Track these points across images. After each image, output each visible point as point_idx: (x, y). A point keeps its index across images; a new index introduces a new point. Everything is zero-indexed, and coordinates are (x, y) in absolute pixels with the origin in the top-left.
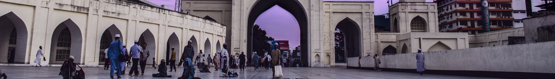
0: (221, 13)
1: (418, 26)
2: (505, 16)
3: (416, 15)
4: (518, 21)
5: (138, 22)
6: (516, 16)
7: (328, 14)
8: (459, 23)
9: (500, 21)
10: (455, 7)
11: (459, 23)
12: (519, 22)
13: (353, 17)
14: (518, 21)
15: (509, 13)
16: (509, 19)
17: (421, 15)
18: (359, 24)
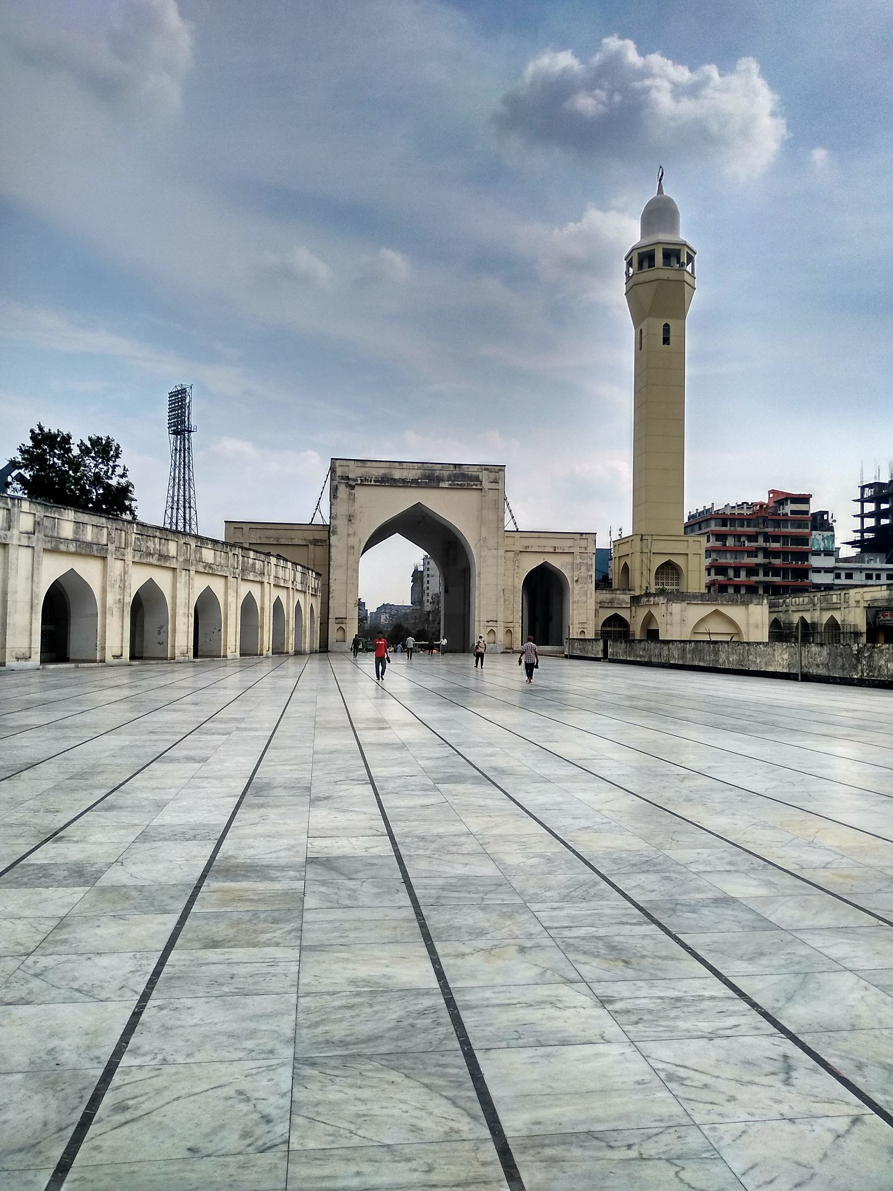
0: (306, 548)
1: (667, 579)
2: (797, 560)
3: (664, 559)
4: (818, 570)
5: (192, 573)
6: (816, 562)
7: (511, 554)
8: (713, 572)
9: (786, 570)
10: (708, 541)
11: (713, 572)
12: (820, 572)
13: (556, 562)
14: (818, 570)
15: (804, 556)
16: (803, 566)
17: (674, 559)
18: (567, 573)
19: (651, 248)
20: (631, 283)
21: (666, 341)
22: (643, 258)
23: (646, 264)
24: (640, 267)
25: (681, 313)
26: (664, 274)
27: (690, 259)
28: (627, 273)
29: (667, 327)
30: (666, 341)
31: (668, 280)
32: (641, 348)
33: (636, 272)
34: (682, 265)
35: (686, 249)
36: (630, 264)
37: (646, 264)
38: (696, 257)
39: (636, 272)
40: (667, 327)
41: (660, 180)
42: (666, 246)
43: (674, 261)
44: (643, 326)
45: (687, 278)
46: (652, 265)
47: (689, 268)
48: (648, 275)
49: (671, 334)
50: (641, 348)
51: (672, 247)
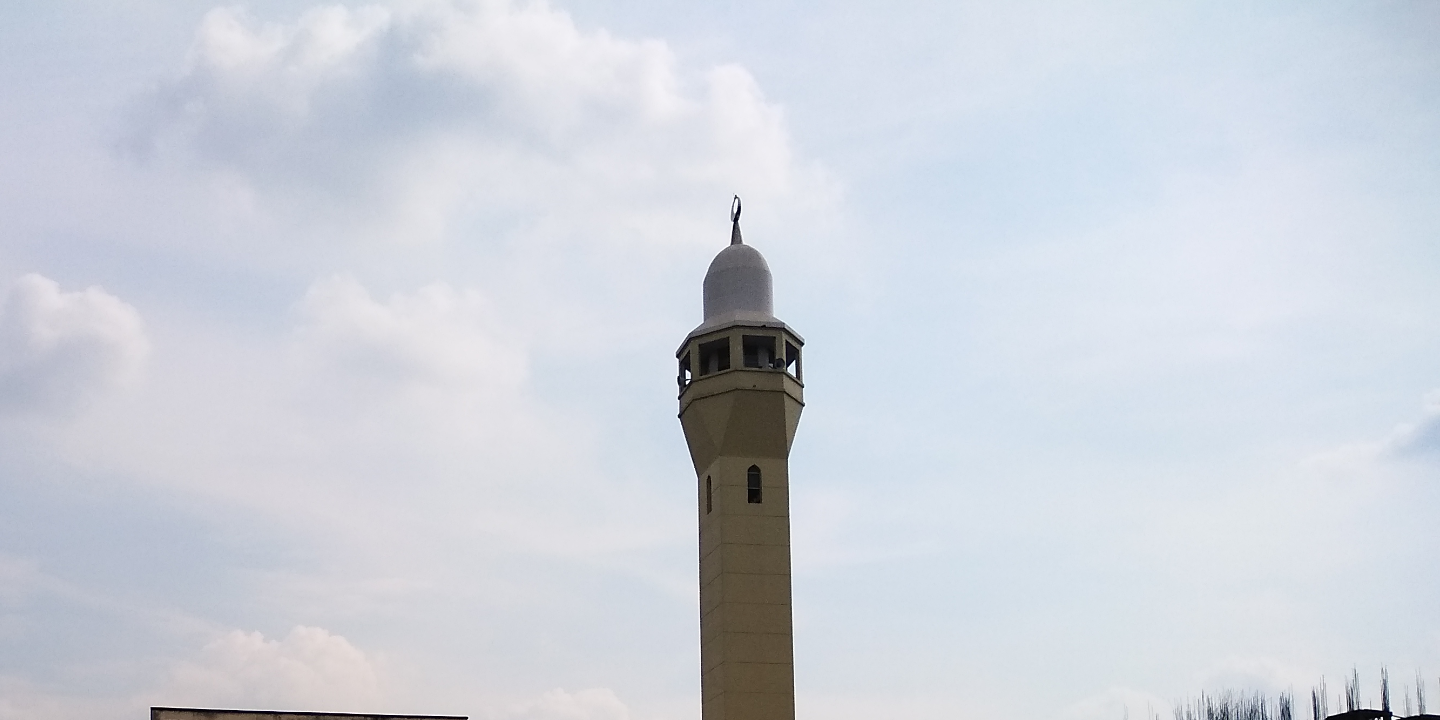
21: (754, 496)
22: (703, 355)
23: (714, 364)
24: (704, 368)
25: (782, 450)
26: (747, 380)
27: (794, 354)
28: (681, 380)
29: (754, 474)
30: (754, 496)
31: (754, 390)
32: (709, 510)
33: (697, 377)
34: (779, 366)
35: (785, 337)
36: (685, 365)
37: (714, 364)
38: (804, 352)
39: (697, 377)
40: (754, 474)
41: (736, 220)
42: (748, 332)
43: (763, 359)
44: (713, 470)
45: (788, 386)
46: (724, 364)
47: (792, 369)
48: (718, 383)
49: (764, 483)
50: (709, 510)
51: (760, 333)
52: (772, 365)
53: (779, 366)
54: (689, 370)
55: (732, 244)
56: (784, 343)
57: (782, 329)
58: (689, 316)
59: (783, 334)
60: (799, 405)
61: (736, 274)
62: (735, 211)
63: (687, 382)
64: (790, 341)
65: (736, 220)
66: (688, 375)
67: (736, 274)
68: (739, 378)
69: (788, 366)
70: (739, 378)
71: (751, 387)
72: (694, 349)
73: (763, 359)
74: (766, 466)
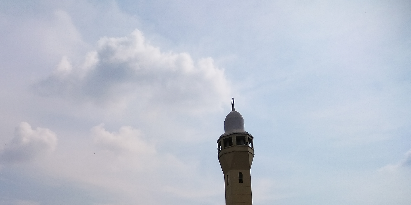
19: (230, 136)
20: (221, 153)
21: (241, 181)
23: (228, 144)
24: (225, 145)
25: (248, 167)
26: (238, 148)
28: (219, 149)
29: (241, 174)
30: (241, 181)
32: (228, 185)
34: (247, 144)
35: (248, 136)
36: (219, 145)
37: (228, 144)
40: (241, 174)
41: (233, 104)
42: (237, 135)
43: (242, 142)
45: (250, 150)
46: (231, 144)
47: (250, 145)
48: (229, 149)
50: (228, 185)
52: (244, 144)
53: (246, 144)
54: (221, 146)
55: (232, 111)
56: (248, 138)
57: (247, 134)
58: (221, 132)
59: (248, 135)
60: (253, 155)
61: (233, 119)
62: (233, 102)
63: (220, 149)
64: (249, 137)
65: (233, 104)
66: (221, 147)
67: (233, 119)
68: (235, 148)
69: (249, 144)
70: (235, 148)
71: (239, 150)
72: (222, 140)
73: (242, 142)
74: (244, 172)
